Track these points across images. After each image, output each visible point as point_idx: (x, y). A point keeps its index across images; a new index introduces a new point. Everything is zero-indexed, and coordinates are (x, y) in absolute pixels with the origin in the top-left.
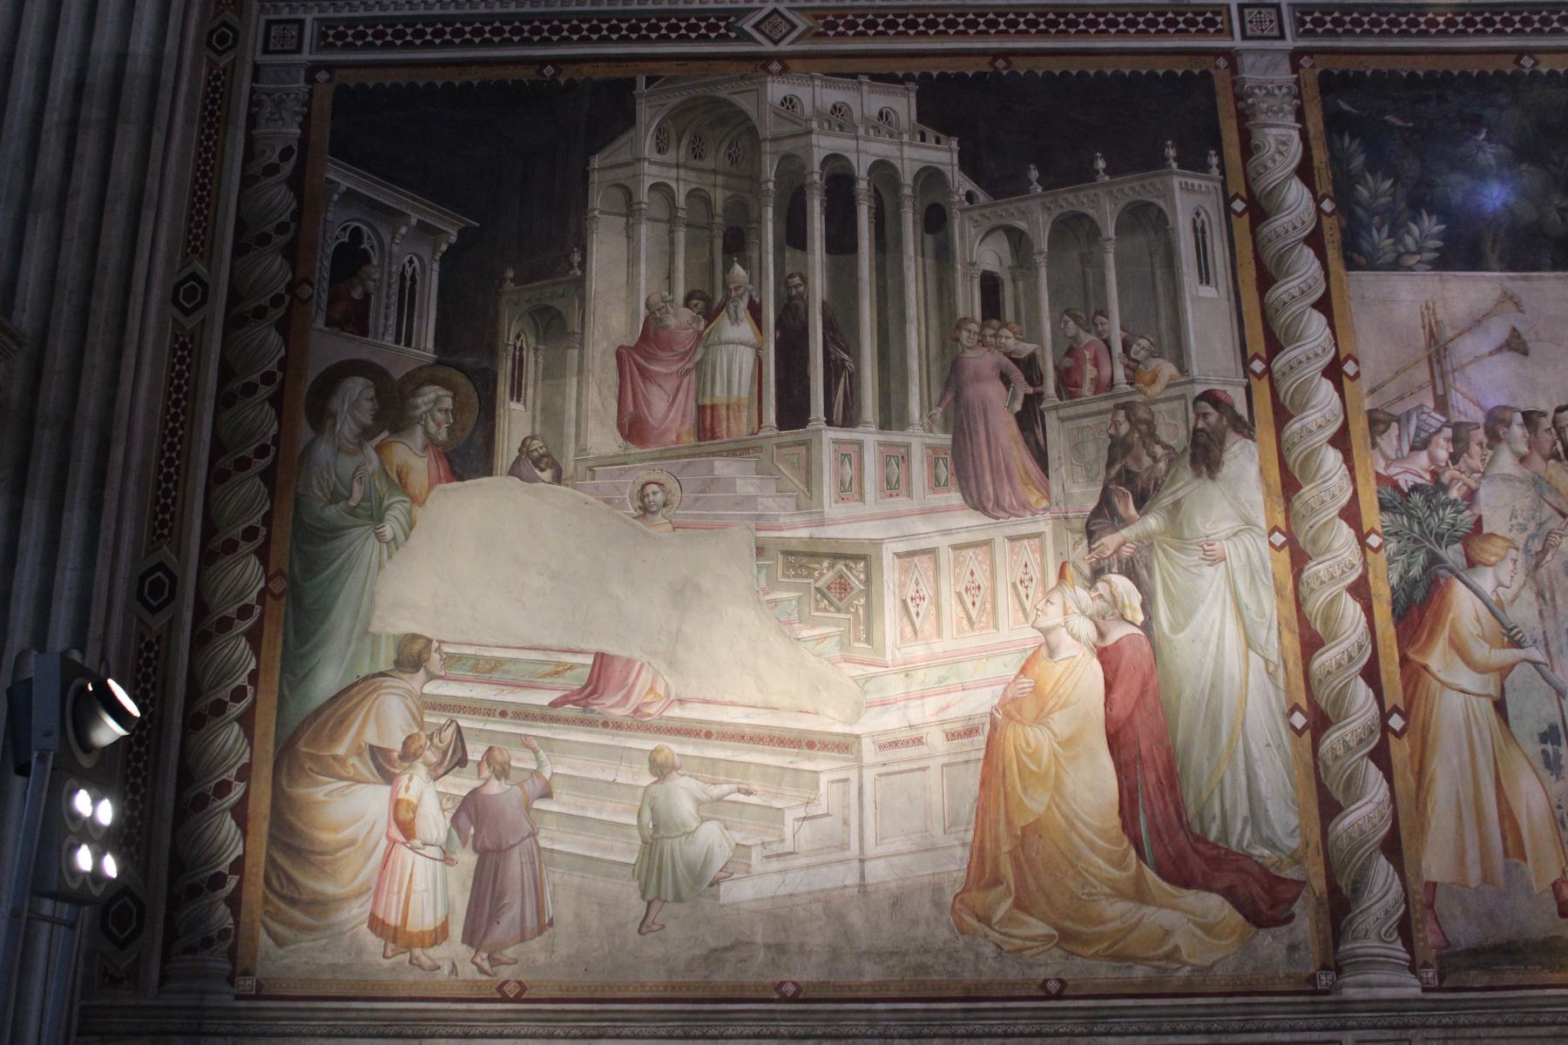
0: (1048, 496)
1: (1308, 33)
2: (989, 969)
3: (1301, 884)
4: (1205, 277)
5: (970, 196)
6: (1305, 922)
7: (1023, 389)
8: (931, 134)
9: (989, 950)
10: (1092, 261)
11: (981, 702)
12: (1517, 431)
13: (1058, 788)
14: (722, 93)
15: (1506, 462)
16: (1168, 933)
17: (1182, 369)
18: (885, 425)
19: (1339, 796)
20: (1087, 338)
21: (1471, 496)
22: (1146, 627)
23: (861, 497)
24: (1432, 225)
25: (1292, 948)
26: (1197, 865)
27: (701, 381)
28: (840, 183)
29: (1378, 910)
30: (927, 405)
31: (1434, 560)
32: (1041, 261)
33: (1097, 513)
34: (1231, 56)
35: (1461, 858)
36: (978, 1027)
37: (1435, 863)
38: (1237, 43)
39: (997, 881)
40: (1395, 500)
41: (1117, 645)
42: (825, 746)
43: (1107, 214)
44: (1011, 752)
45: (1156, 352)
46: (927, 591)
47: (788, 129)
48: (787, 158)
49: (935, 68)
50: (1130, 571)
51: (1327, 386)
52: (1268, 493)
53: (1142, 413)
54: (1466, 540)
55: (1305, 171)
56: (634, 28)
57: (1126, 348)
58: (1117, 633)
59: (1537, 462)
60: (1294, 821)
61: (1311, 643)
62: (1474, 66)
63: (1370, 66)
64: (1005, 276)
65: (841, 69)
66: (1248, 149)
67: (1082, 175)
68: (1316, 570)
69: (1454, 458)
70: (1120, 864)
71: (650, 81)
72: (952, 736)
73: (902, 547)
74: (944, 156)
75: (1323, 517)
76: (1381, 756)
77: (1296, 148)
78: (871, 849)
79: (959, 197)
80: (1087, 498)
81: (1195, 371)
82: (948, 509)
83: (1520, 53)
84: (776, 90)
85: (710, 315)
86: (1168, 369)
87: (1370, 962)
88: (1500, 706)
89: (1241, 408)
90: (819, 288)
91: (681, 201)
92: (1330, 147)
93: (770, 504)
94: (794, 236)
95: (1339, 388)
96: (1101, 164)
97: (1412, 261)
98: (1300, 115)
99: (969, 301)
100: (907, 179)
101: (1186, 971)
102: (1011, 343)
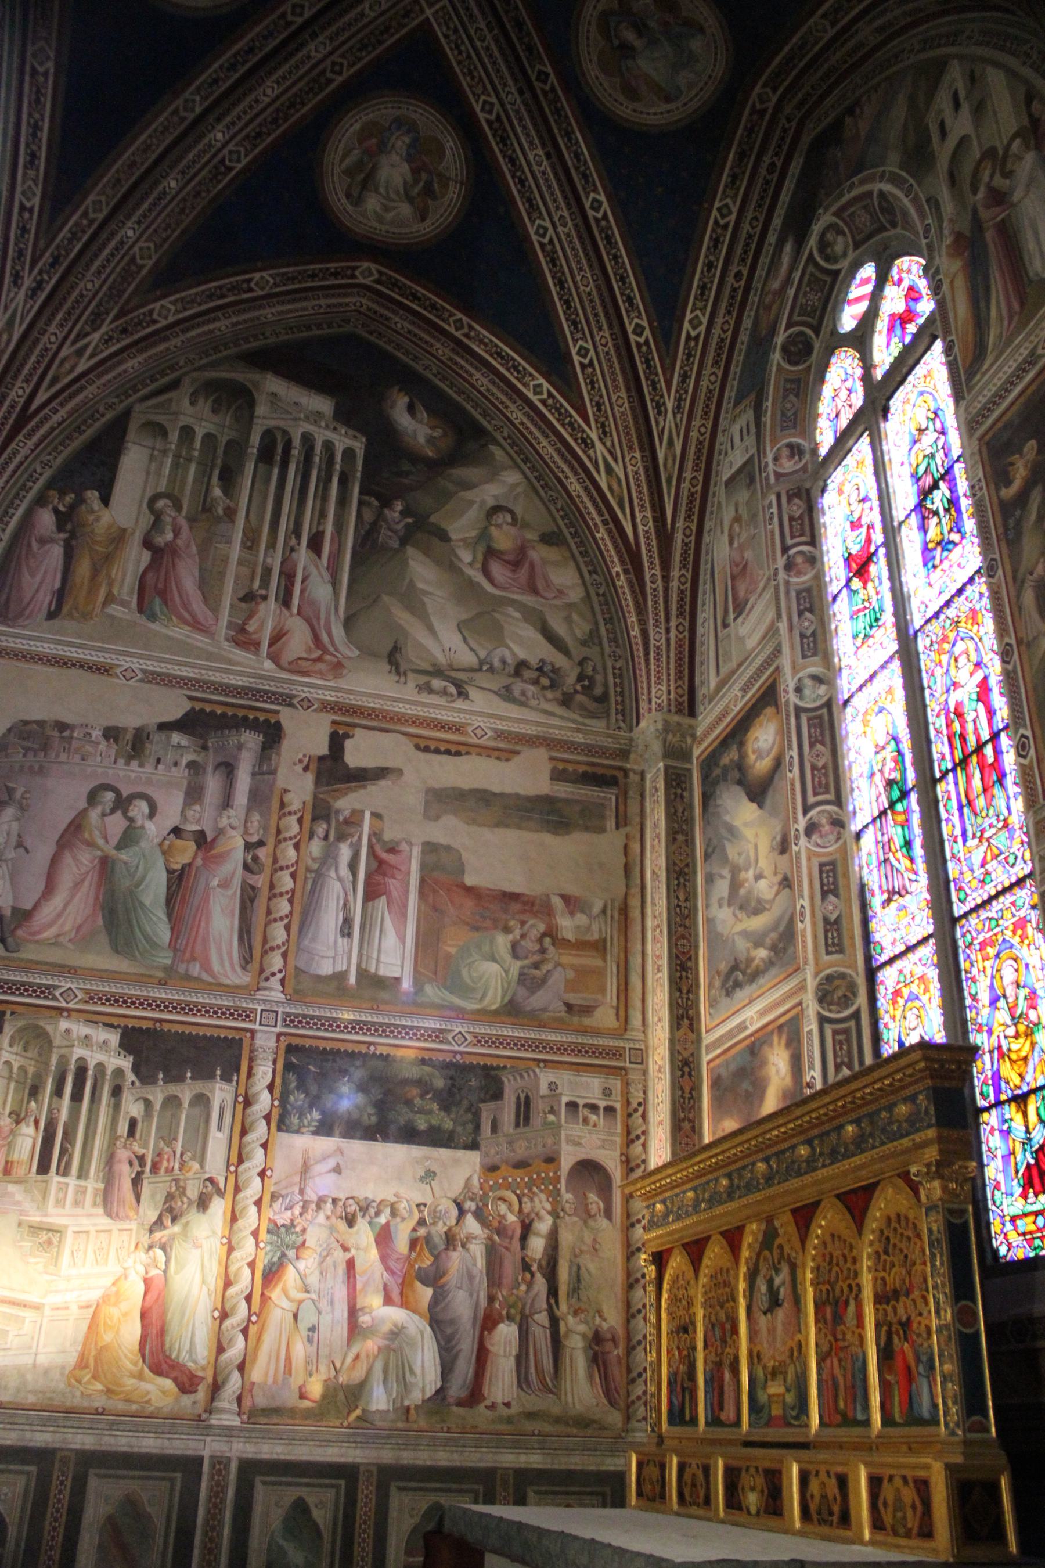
0: (137, 1213)
1: (287, 1026)
2: (77, 1401)
3: (203, 1378)
4: (220, 1128)
5: (133, 1083)
6: (201, 1394)
7: (137, 1168)
8: (123, 1053)
9: (78, 1394)
10: (175, 1117)
11: (95, 1295)
12: (329, 1206)
13: (118, 1332)
14: (41, 1023)
15: (321, 1218)
16: (148, 1393)
17: (202, 1167)
18: (79, 1177)
19: (225, 1345)
20: (167, 1149)
21: (304, 1230)
22: (165, 1271)
23: (64, 1206)
24: (316, 1115)
25: (195, 1403)
26: (165, 1367)
27: (9, 1151)
28: (81, 1071)
29: (230, 1391)
30: (97, 1171)
31: (284, 1255)
32: (156, 1114)
33: (155, 1223)
34: (253, 1032)
35: (266, 1374)
36: (69, 1423)
37: (256, 1374)
38: (257, 1027)
39: (86, 1367)
40: (274, 1229)
41: (151, 1279)
42: (30, 1307)
43: (186, 1098)
44: (102, 1316)
45: (193, 1159)
46: (82, 1247)
47: (66, 1043)
48: (62, 1057)
49: (131, 1023)
50: (163, 1248)
51: (258, 1179)
52: (225, 1221)
53: (182, 1184)
54: (298, 1249)
55: (271, 1087)
56: (10, 988)
57: (182, 1155)
58: (153, 1272)
59: (334, 1220)
60: (206, 1353)
61: (228, 1284)
62: (350, 1047)
63: (308, 1043)
64: (140, 1119)
65: (92, 1019)
66: (250, 1074)
67: (181, 1079)
68: (236, 1254)
69: (301, 1215)
70: (135, 1364)
71: (12, 1013)
72: (81, 1307)
73: (76, 1229)
74: (126, 1063)
75: (244, 1234)
76: (245, 1332)
77: (270, 1076)
78: (41, 1349)
79: (128, 1083)
80: (153, 1216)
81: (207, 1168)
82: (97, 1215)
83: (370, 1044)
84: (64, 1024)
85: (18, 1122)
86: (196, 1166)
87: (223, 1411)
88: (295, 1316)
89: (222, 1186)
90: (64, 1116)
91: (15, 1070)
92: (284, 1079)
93: (27, 1206)
94: (58, 1092)
95: (263, 1181)
96: (189, 1075)
97: (304, 1130)
98: (274, 1062)
99: (123, 1128)
100: (109, 1072)
101: (151, 1409)
102: (136, 1147)
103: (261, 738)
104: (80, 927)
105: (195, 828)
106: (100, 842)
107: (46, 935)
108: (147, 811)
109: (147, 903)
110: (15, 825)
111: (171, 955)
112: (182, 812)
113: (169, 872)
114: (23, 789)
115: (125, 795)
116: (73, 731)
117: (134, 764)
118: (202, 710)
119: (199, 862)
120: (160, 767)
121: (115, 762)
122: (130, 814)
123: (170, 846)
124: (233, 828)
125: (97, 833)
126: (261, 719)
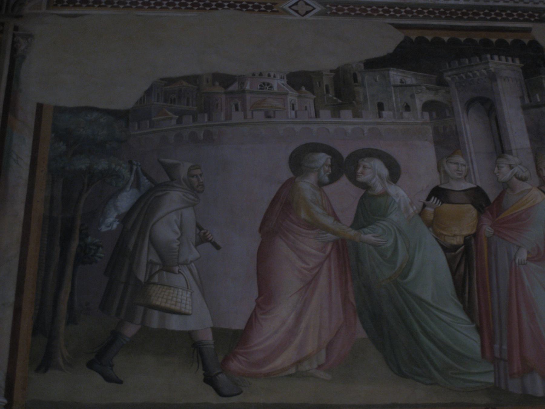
103: (517, 61)
104: (330, 346)
105: (467, 185)
106: (328, 221)
107: (279, 362)
108: (385, 172)
109: (427, 296)
110: (189, 214)
111: (492, 368)
112: (439, 168)
113: (446, 249)
114: (189, 165)
115: (345, 156)
116: (242, 84)
117: (347, 115)
118: (421, 40)
119: (487, 230)
120: (385, 113)
121: (317, 115)
122: (362, 179)
123: (436, 214)
124: (523, 179)
125: (317, 209)
126: (509, 41)
